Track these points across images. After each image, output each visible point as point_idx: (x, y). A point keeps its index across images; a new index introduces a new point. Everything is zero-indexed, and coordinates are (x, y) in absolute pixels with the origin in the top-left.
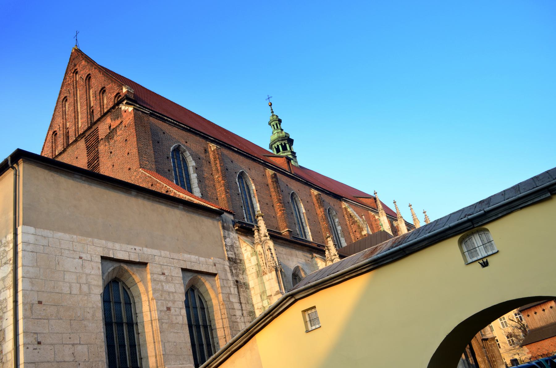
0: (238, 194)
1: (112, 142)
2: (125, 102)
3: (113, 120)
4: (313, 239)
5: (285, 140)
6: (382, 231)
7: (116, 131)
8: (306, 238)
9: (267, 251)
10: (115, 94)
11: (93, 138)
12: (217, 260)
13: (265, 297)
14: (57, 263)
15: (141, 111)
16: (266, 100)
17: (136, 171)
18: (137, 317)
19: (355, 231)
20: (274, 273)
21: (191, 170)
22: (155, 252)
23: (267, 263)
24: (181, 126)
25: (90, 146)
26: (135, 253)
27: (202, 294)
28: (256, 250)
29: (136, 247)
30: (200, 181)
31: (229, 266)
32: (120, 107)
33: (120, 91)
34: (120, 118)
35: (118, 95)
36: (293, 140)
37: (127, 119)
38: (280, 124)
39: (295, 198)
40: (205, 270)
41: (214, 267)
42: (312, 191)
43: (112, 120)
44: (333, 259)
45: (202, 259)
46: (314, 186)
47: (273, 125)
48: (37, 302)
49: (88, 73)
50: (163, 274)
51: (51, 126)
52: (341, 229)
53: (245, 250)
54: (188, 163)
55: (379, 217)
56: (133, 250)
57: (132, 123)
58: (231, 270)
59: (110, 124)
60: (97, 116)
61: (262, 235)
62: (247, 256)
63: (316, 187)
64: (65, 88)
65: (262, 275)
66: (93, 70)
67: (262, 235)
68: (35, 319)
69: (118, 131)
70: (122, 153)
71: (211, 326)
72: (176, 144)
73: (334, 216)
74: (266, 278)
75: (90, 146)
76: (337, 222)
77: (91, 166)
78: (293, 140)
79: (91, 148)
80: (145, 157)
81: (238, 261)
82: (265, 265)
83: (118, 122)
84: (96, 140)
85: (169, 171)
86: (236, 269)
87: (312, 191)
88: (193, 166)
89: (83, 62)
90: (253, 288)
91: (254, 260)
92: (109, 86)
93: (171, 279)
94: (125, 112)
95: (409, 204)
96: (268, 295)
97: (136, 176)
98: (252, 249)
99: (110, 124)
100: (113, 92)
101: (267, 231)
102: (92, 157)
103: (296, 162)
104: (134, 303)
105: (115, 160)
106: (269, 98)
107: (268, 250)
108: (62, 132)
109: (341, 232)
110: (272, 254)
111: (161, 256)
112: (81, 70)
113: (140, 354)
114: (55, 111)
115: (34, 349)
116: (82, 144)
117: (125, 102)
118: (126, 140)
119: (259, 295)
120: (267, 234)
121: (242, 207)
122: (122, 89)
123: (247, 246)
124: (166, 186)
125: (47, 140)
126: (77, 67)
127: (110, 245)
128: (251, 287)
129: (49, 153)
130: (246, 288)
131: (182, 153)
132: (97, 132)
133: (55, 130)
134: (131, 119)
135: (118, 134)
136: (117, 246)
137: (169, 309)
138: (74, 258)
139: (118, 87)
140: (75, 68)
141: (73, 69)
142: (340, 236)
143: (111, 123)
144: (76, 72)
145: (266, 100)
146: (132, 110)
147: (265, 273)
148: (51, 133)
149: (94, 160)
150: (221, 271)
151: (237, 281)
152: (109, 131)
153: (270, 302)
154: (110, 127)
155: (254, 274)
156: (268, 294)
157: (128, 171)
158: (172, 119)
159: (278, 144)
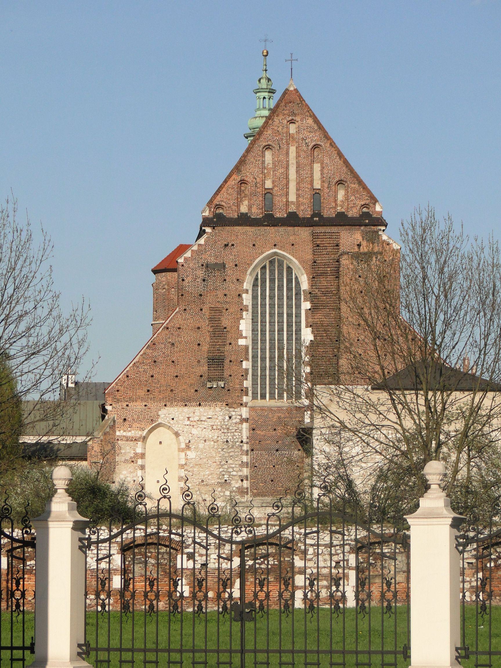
10: (363, 203)
25: (322, 245)
33: (371, 205)
43: (363, 239)
49: (319, 143)
51: (237, 169)
60: (328, 213)
64: (270, 132)
75: (322, 245)
106: (265, 41)
112: (304, 130)
125: (228, 183)
141: (289, 116)
143: (361, 240)
154: (359, 245)
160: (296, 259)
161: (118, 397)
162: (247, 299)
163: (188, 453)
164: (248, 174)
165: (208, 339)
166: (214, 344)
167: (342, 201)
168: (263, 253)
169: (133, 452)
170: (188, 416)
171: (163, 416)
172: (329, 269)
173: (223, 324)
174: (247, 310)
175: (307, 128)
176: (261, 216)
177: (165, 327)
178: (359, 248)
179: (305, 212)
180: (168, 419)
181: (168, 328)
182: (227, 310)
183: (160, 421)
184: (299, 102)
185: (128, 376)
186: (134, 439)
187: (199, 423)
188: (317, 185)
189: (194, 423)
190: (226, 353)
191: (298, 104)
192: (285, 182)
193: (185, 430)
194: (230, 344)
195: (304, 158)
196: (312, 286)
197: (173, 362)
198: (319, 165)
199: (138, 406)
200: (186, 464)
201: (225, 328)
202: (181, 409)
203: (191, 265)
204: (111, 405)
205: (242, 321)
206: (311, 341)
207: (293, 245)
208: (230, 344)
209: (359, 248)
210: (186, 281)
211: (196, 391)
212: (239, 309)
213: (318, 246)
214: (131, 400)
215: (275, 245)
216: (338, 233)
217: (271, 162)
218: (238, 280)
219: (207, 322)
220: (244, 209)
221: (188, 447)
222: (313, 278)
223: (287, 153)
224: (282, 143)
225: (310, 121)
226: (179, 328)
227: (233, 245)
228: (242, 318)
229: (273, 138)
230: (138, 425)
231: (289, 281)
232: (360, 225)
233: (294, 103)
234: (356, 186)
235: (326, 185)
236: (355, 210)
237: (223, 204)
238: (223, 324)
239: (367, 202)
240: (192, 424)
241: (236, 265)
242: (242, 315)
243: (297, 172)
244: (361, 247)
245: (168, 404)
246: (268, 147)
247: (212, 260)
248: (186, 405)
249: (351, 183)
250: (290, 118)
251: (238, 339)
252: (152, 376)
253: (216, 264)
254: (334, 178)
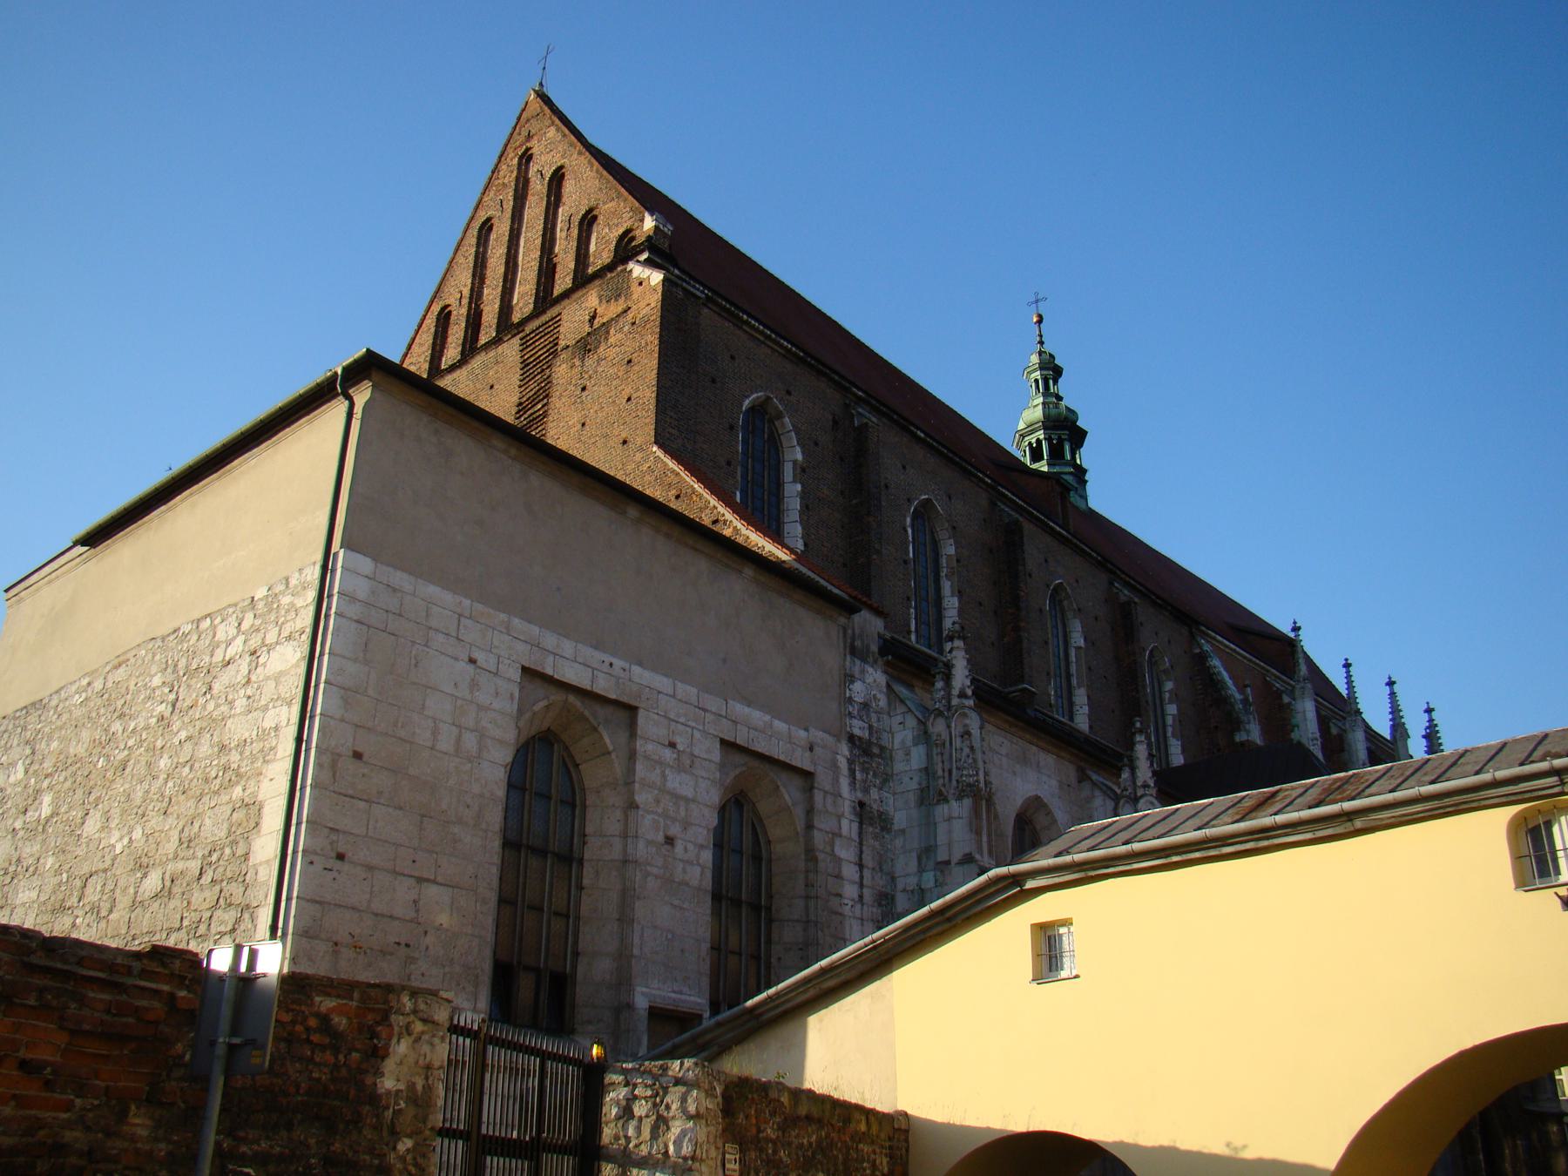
0: (905, 562)
1: (590, 362)
2: (645, 256)
3: (604, 301)
4: (1091, 727)
5: (1063, 430)
6: (1295, 742)
7: (608, 332)
8: (1071, 719)
9: (959, 740)
10: (621, 231)
11: (542, 340)
12: (818, 735)
13: (931, 864)
14: (413, 662)
15: (685, 290)
16: (1029, 304)
17: (641, 449)
18: (584, 843)
19: (1216, 727)
20: (967, 802)
21: (788, 472)
22: (661, 682)
23: (954, 771)
24: (781, 346)
25: (532, 359)
26: (609, 674)
27: (761, 820)
28: (931, 729)
29: (615, 661)
30: (807, 507)
31: (848, 760)
32: (628, 270)
34: (623, 298)
35: (627, 236)
36: (1087, 433)
37: (642, 304)
38: (1056, 382)
39: (1061, 601)
40: (782, 758)
41: (808, 754)
42: (1115, 591)
43: (601, 301)
44: (1139, 794)
45: (780, 725)
46: (1123, 576)
47: (1036, 381)
48: (351, 753)
49: (559, 164)
50: (672, 745)
52: (1175, 712)
53: (900, 724)
54: (783, 452)
55: (1294, 699)
56: (605, 667)
57: (656, 316)
58: (852, 772)
59: (596, 310)
61: (955, 692)
62: (903, 742)
63: (1127, 579)
64: (492, 194)
65: (935, 800)
66: (575, 156)
67: (955, 692)
68: (340, 794)
69: (612, 331)
70: (613, 393)
71: (769, 909)
72: (759, 394)
73: (1164, 671)
74: (941, 811)
75: (532, 359)
76: (1170, 691)
77: (526, 416)
78: (1087, 433)
79: (535, 366)
80: (671, 417)
81: (876, 750)
82: (946, 774)
83: (615, 308)
84: (551, 348)
85: (729, 463)
86: (865, 770)
87: (1115, 591)
88: (795, 462)
89: (552, 133)
90: (903, 831)
91: (918, 756)
92: (610, 205)
93: (688, 762)
94: (641, 284)
95: (1390, 678)
96: (939, 859)
97: (638, 465)
98: (918, 724)
99: (593, 309)
100: (617, 225)
101: (969, 684)
102: (532, 390)
103: (1085, 498)
104: (584, 807)
105: (591, 411)
106: (1037, 301)
107: (962, 737)
108: (464, 311)
109: (1174, 720)
110: (972, 748)
111: (674, 696)
113: (576, 942)
114: (457, 250)
115: (325, 869)
116: (511, 349)
117: (645, 256)
118: (629, 361)
119: (914, 854)
120: (969, 692)
121: (908, 599)
122: (642, 220)
123: (907, 712)
124: (714, 506)
125: (424, 325)
126: (533, 143)
127: (550, 640)
128: (896, 827)
129: (422, 361)
130: (883, 829)
131: (771, 421)
132: (556, 325)
133: (447, 302)
134: (653, 305)
135: (612, 340)
136: (568, 647)
137: (670, 841)
138: (456, 659)
139: (631, 214)
140: (528, 145)
141: (521, 145)
142: (1169, 734)
145: (1029, 304)
146: (659, 283)
147: (942, 798)
148: (436, 309)
149: (534, 400)
150: (825, 768)
151: (861, 804)
152: (587, 329)
153: (941, 880)
154: (593, 317)
155: (911, 794)
156: (942, 856)
157: (620, 446)
158: (761, 323)
159: (1042, 437)
164: (452, 290)
213: (528, 364)
249: (604, 203)
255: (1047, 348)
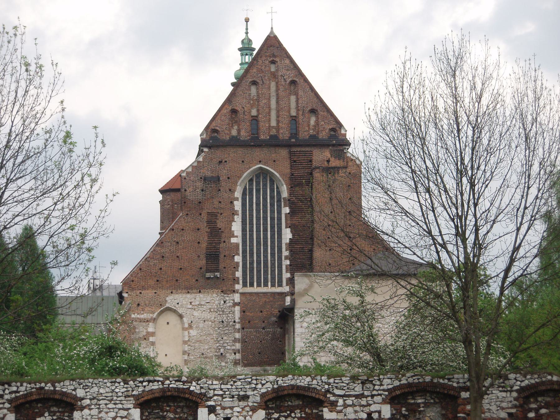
10: (330, 127)
33: (337, 129)
35: (333, 130)
43: (331, 156)
49: (295, 79)
60: (304, 135)
64: (255, 70)
69: (340, 171)
79: (299, 165)
116: (284, 153)
125: (222, 112)
133: (236, 108)
141: (270, 57)
144: (273, 62)
154: (328, 161)
160: (277, 172)
161: (133, 286)
162: (238, 205)
163: (191, 331)
164: (237, 104)
165: (206, 238)
166: (211, 242)
167: (314, 126)
168: (250, 168)
169: (145, 331)
170: (190, 301)
171: (169, 301)
172: (304, 181)
173: (218, 226)
174: (238, 215)
175: (285, 67)
176: (249, 138)
177: (171, 229)
178: (328, 163)
179: (284, 134)
180: (174, 304)
181: (173, 230)
182: (221, 214)
183: (167, 305)
184: (278, 46)
185: (140, 269)
186: (146, 321)
187: (199, 306)
188: (293, 113)
189: (196, 307)
190: (221, 249)
191: (278, 47)
192: (267, 110)
193: (188, 312)
194: (224, 242)
195: (283, 91)
196: (290, 194)
197: (178, 257)
198: (295, 97)
199: (149, 294)
200: (189, 340)
201: (220, 229)
202: (184, 296)
203: (192, 178)
204: (127, 293)
205: (233, 224)
206: (290, 239)
207: (274, 161)
208: (224, 242)
209: (328, 163)
210: (188, 191)
211: (197, 280)
212: (231, 214)
214: (144, 288)
215: (260, 162)
216: (311, 151)
217: (256, 94)
218: (230, 190)
219: (205, 224)
220: (234, 132)
221: (190, 327)
222: (291, 188)
223: (269, 88)
224: (265, 79)
225: (287, 61)
226: (183, 230)
227: (226, 162)
228: (233, 221)
229: (257, 75)
230: (150, 309)
231: (272, 191)
232: (328, 146)
233: (274, 47)
234: (325, 113)
235: (301, 113)
236: (324, 133)
237: (217, 128)
238: (218, 226)
239: (334, 126)
240: (193, 307)
241: (228, 178)
242: (234, 218)
243: (277, 102)
244: (330, 163)
245: (174, 291)
246: (254, 83)
247: (209, 174)
248: (188, 292)
250: (271, 59)
251: (230, 237)
252: (161, 269)
253: (212, 176)
254: (307, 107)
255: (250, 36)
